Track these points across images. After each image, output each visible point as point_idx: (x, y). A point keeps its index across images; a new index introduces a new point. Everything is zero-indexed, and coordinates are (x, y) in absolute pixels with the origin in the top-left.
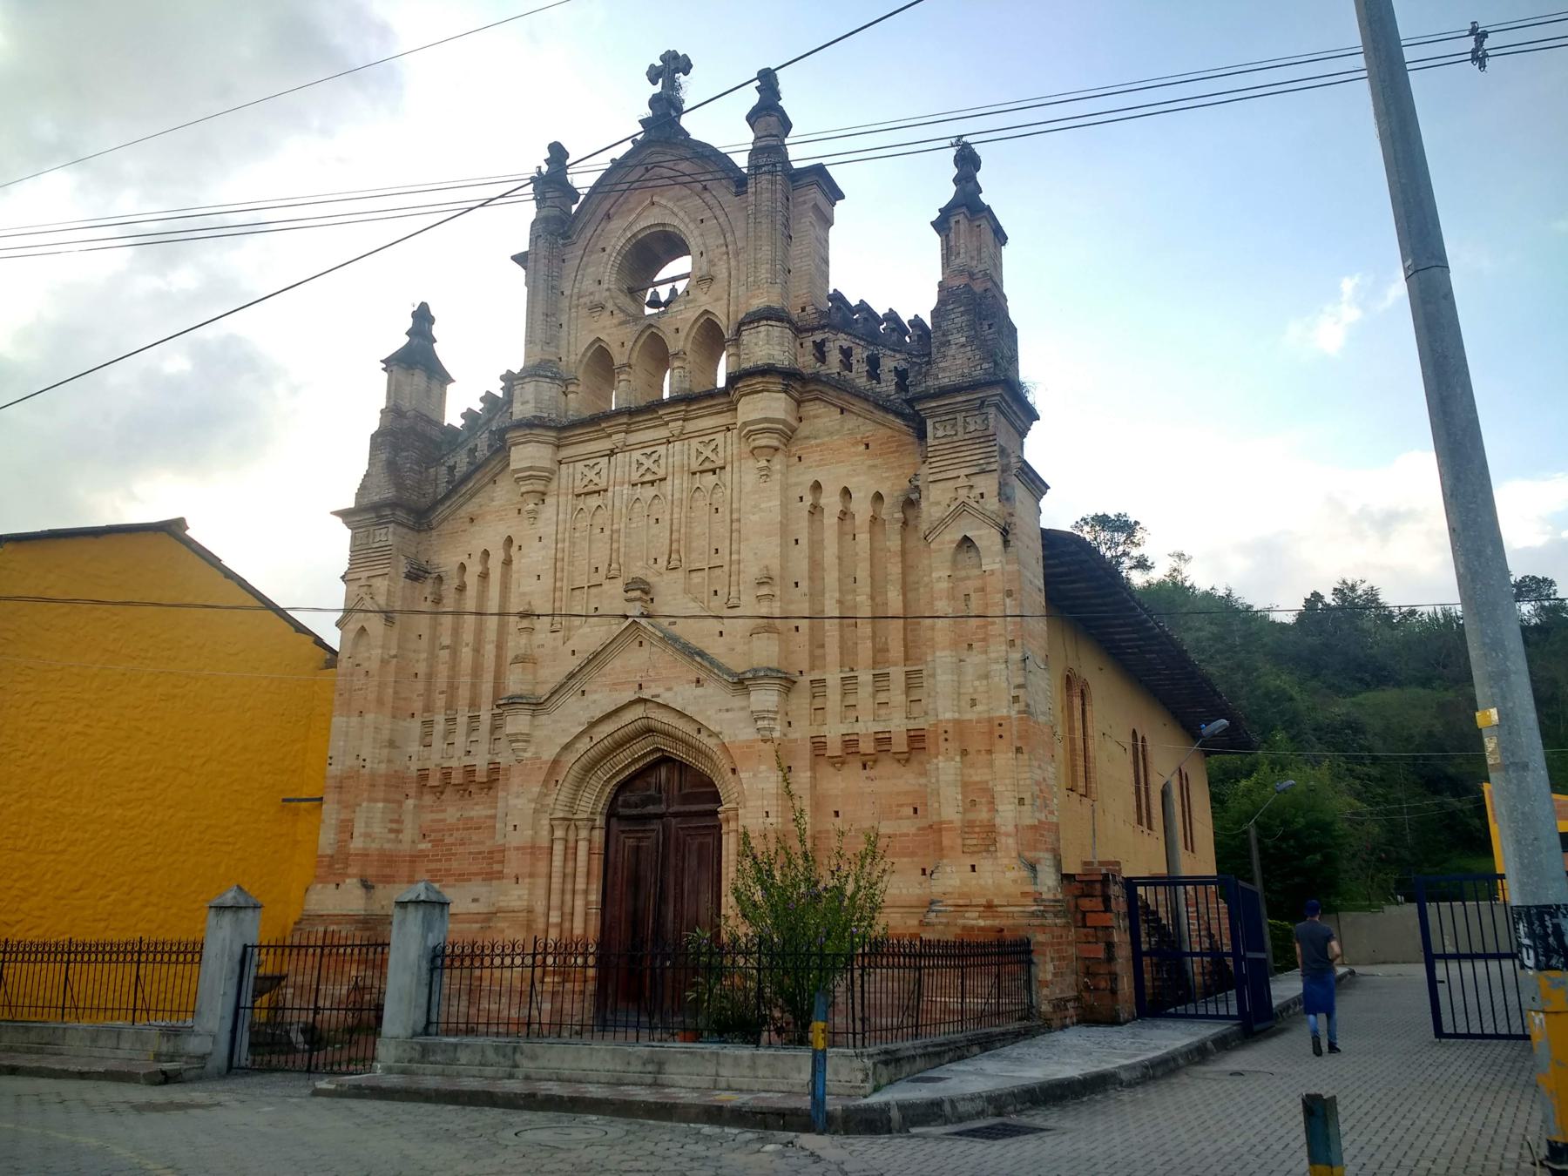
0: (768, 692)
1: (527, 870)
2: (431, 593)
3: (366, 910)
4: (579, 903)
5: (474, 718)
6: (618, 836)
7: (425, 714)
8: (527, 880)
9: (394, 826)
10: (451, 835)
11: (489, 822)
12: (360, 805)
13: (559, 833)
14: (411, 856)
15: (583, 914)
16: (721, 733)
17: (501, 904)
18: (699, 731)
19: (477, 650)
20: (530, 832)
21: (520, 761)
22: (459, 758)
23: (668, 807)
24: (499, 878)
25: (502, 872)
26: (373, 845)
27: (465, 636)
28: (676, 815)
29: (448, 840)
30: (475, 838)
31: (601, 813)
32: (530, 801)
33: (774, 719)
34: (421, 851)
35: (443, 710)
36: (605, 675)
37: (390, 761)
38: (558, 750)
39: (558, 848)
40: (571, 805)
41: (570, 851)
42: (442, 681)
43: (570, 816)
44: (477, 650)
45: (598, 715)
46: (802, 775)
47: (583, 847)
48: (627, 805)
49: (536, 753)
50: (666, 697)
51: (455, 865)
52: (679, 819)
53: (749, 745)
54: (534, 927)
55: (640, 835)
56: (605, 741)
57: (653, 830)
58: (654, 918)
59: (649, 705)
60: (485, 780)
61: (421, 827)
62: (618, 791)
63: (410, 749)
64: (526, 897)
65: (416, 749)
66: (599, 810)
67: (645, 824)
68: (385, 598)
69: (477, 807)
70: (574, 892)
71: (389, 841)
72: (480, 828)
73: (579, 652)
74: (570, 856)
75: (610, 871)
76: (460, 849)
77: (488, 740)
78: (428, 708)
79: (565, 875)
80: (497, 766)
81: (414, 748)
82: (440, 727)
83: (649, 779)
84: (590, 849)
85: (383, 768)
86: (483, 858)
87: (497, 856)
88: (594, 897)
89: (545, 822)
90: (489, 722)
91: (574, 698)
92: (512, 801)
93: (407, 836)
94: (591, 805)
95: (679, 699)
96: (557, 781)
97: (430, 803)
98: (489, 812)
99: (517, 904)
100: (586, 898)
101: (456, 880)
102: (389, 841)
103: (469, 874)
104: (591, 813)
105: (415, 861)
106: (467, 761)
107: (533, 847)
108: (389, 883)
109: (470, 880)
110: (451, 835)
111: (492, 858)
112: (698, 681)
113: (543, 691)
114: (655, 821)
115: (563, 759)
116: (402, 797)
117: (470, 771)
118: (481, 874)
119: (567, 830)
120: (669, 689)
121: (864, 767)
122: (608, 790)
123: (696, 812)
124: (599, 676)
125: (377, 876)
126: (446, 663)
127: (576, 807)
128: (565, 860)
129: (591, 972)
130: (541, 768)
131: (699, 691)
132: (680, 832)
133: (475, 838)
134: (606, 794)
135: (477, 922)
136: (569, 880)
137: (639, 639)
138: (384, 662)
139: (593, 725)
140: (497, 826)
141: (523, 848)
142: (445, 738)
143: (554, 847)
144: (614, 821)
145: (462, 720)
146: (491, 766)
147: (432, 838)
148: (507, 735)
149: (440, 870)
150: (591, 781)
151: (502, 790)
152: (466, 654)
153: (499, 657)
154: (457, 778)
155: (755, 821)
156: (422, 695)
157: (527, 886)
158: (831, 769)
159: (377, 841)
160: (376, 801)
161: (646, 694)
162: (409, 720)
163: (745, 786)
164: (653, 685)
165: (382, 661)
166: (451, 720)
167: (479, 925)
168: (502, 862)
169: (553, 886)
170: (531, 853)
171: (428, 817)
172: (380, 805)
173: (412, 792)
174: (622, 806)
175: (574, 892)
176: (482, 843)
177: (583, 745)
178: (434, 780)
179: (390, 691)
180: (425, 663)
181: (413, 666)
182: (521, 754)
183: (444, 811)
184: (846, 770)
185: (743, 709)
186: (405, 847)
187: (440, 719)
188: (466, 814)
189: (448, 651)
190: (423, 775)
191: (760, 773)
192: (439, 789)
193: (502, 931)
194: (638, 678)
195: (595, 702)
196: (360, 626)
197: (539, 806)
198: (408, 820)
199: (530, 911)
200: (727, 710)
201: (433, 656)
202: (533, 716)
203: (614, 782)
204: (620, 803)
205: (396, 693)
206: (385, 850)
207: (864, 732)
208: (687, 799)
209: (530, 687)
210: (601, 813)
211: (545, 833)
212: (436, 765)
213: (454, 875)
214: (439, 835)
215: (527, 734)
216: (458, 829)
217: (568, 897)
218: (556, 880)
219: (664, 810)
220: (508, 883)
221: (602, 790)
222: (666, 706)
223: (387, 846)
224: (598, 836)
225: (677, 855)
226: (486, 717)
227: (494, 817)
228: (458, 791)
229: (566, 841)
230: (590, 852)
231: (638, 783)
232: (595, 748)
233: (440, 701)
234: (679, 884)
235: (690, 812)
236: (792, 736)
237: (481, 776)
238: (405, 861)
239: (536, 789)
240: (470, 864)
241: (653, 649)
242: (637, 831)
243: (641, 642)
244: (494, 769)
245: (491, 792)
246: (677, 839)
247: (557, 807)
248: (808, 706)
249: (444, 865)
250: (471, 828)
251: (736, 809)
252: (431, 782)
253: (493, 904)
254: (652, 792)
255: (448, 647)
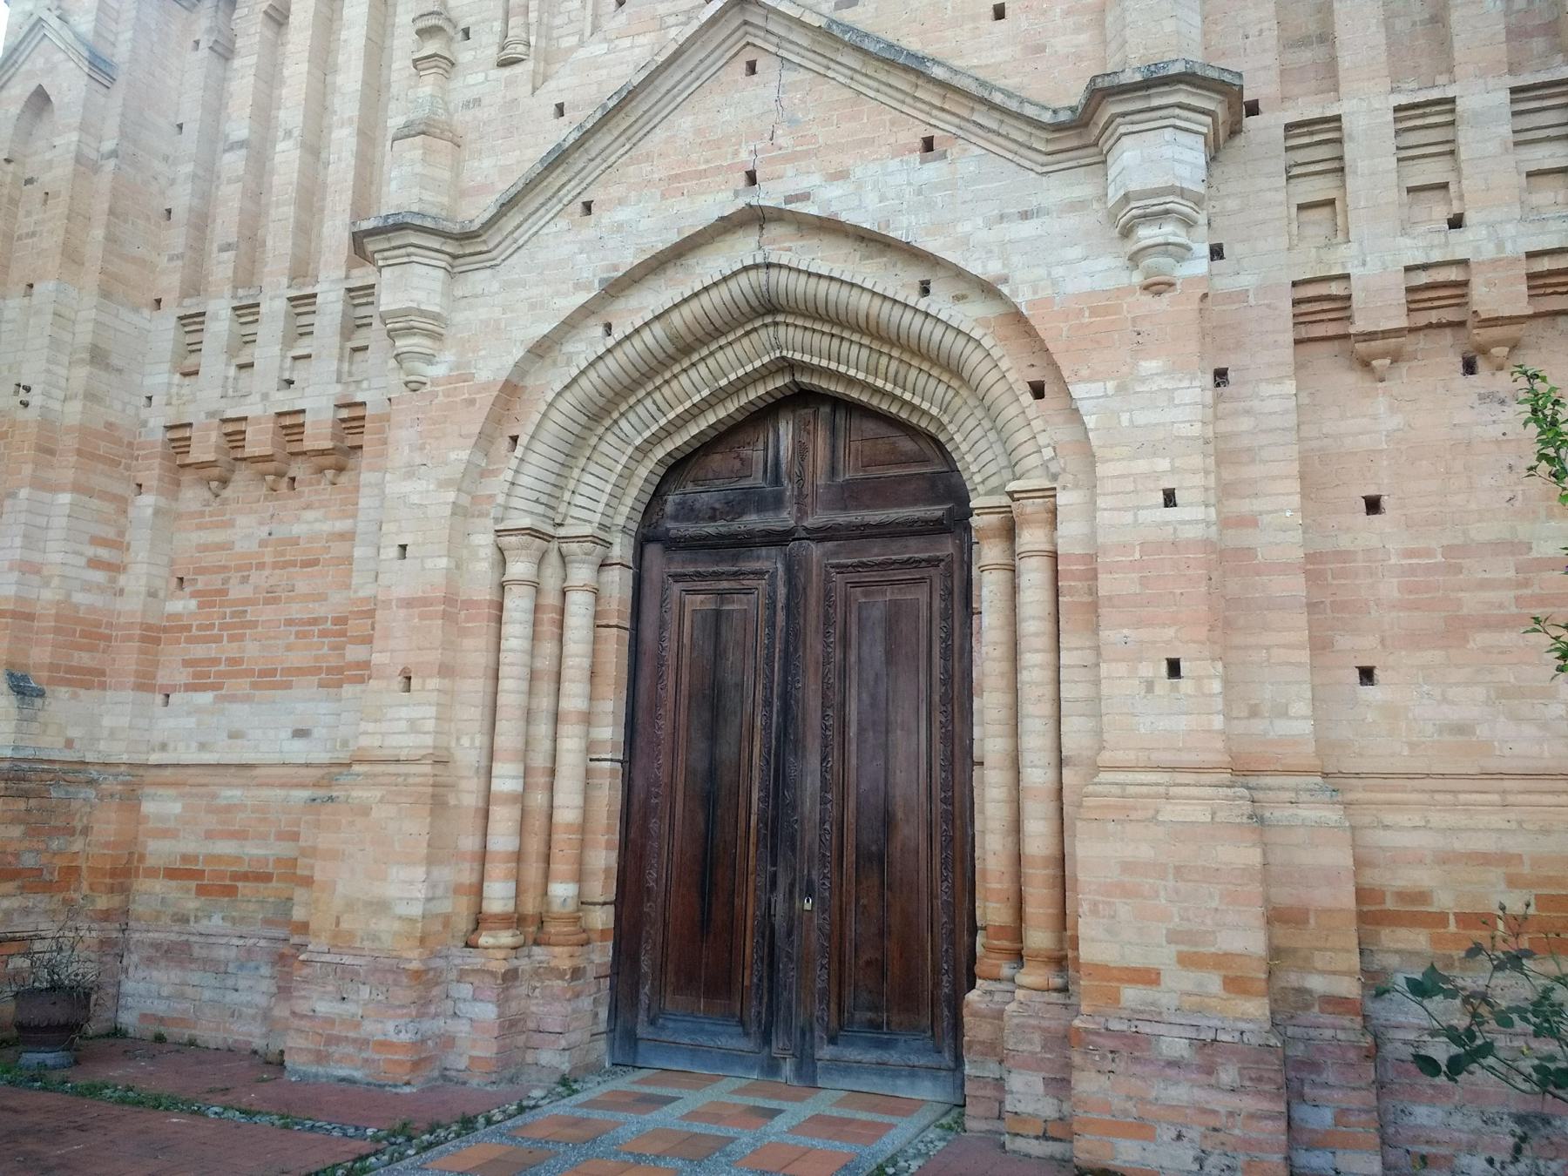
0: (1181, 136)
1: (434, 656)
2: (210, 30)
3: (16, 748)
4: (571, 744)
5: (303, 303)
6: (664, 590)
7: (187, 302)
8: (434, 683)
9: (104, 553)
10: (245, 580)
11: (338, 549)
12: (12, 495)
13: (519, 568)
14: (149, 627)
15: (581, 771)
16: (1005, 280)
17: (364, 741)
18: (925, 291)
19: (314, 150)
20: (443, 562)
21: (415, 386)
22: (265, 396)
23: (802, 513)
24: (361, 680)
25: (366, 665)
26: (47, 595)
27: (282, 114)
28: (823, 534)
29: (236, 591)
30: (302, 587)
31: (624, 530)
32: (443, 484)
33: (1188, 223)
34: (171, 616)
35: (227, 290)
36: (648, 157)
37: (91, 396)
38: (518, 353)
39: (518, 604)
40: (552, 497)
41: (548, 617)
42: (226, 225)
43: (550, 530)
44: (314, 150)
45: (629, 259)
46: (1266, 389)
47: (579, 607)
48: (687, 512)
49: (458, 366)
50: (830, 200)
51: (251, 649)
52: (829, 545)
53: (1102, 305)
54: (452, 802)
55: (725, 585)
56: (646, 335)
57: (759, 574)
58: (764, 788)
59: (773, 230)
60: (328, 444)
61: (172, 562)
62: (664, 479)
63: (148, 381)
64: (430, 725)
65: (164, 378)
66: (620, 520)
67: (735, 559)
68: (92, 17)
69: (309, 515)
70: (556, 718)
71: (87, 587)
72: (314, 563)
73: (575, 107)
74: (548, 629)
75: (646, 671)
76: (267, 613)
77: (336, 351)
78: (194, 286)
79: (533, 676)
80: (357, 412)
81: (159, 377)
82: (220, 324)
83: (746, 452)
84: (596, 615)
85: (73, 412)
86: (323, 634)
87: (356, 627)
88: (609, 732)
89: (484, 541)
90: (339, 307)
91: (562, 223)
92: (396, 486)
93: (136, 580)
94: (600, 507)
95: (871, 200)
96: (515, 439)
97: (195, 506)
98: (342, 525)
99: (404, 743)
100: (588, 733)
101: (254, 686)
102: (87, 587)
103: (289, 671)
104: (602, 527)
105: (157, 641)
106: (285, 401)
107: (449, 600)
108: (88, 686)
109: (288, 686)
110: (245, 580)
111: (343, 634)
112: (928, 144)
113: (476, 212)
114: (764, 551)
115: (530, 382)
116: (129, 491)
117: (290, 425)
118: (315, 671)
119: (541, 561)
120: (841, 175)
121: (1470, 367)
122: (643, 472)
123: (880, 525)
124: (632, 161)
125: (53, 667)
126: (238, 179)
127: (562, 508)
128: (535, 637)
129: (601, 918)
130: (472, 402)
131: (933, 171)
132: (837, 578)
133: (302, 587)
134: (638, 482)
135: (303, 786)
136: (546, 687)
137: (749, 54)
138: (85, 165)
139: (618, 287)
140: (358, 553)
141: (424, 602)
142: (231, 352)
143: (508, 603)
144: (653, 552)
145: (274, 306)
146: (345, 413)
147: (200, 586)
148: (383, 318)
149: (215, 661)
150: (604, 447)
151: (372, 469)
152: (286, 156)
153: (367, 135)
154: (258, 442)
155: (1128, 517)
156: (180, 257)
157: (434, 697)
158: (1352, 379)
159: (55, 582)
160: (55, 488)
161: (769, 196)
162: (146, 312)
163: (1090, 421)
164: (789, 170)
165: (79, 159)
166: (247, 311)
167: (305, 794)
168: (368, 640)
169: (503, 699)
170: (445, 616)
171: (190, 539)
172: (65, 498)
173: (151, 472)
174: (675, 518)
175: (556, 718)
176: (321, 597)
177: (586, 345)
178: (204, 448)
179: (98, 233)
180: (189, 187)
181: (162, 193)
182: (421, 366)
183: (230, 524)
184: (1403, 381)
185: (1077, 206)
186: (132, 606)
187: (220, 310)
188: (281, 531)
189: (243, 152)
190: (179, 436)
191: (1143, 380)
192: (215, 472)
193: (365, 811)
194: (744, 155)
195: (619, 227)
196: (32, 86)
197: (465, 500)
198: (140, 542)
199: (441, 761)
200: (1025, 216)
201: (207, 176)
202: (450, 273)
203: (660, 453)
204: (669, 508)
205: (111, 238)
206: (76, 607)
207: (1489, 251)
208: (850, 495)
209: (445, 200)
210: (624, 530)
211: (482, 566)
212: (211, 415)
213: (249, 673)
214: (216, 581)
215: (436, 317)
216: (261, 566)
217: (543, 729)
218: (512, 687)
219: (792, 523)
220: (384, 689)
221: (627, 474)
222: (829, 227)
223: (79, 598)
224: (618, 583)
225: (826, 634)
226: (332, 296)
227: (348, 537)
228: (263, 475)
229: (537, 587)
230: (598, 624)
231: (716, 461)
232: (618, 353)
233: (222, 267)
234: (835, 706)
235: (867, 525)
236: (1224, 284)
237: (318, 435)
238: (129, 638)
239: (460, 455)
240: (289, 648)
241: (790, 76)
242: (717, 576)
243: (752, 68)
244: (352, 419)
245: (344, 479)
246: (827, 595)
247: (516, 502)
248: (1281, 196)
249: (229, 649)
250: (293, 564)
251: (1050, 493)
252: (197, 454)
253: (345, 743)
254: (757, 480)
255: (242, 144)
